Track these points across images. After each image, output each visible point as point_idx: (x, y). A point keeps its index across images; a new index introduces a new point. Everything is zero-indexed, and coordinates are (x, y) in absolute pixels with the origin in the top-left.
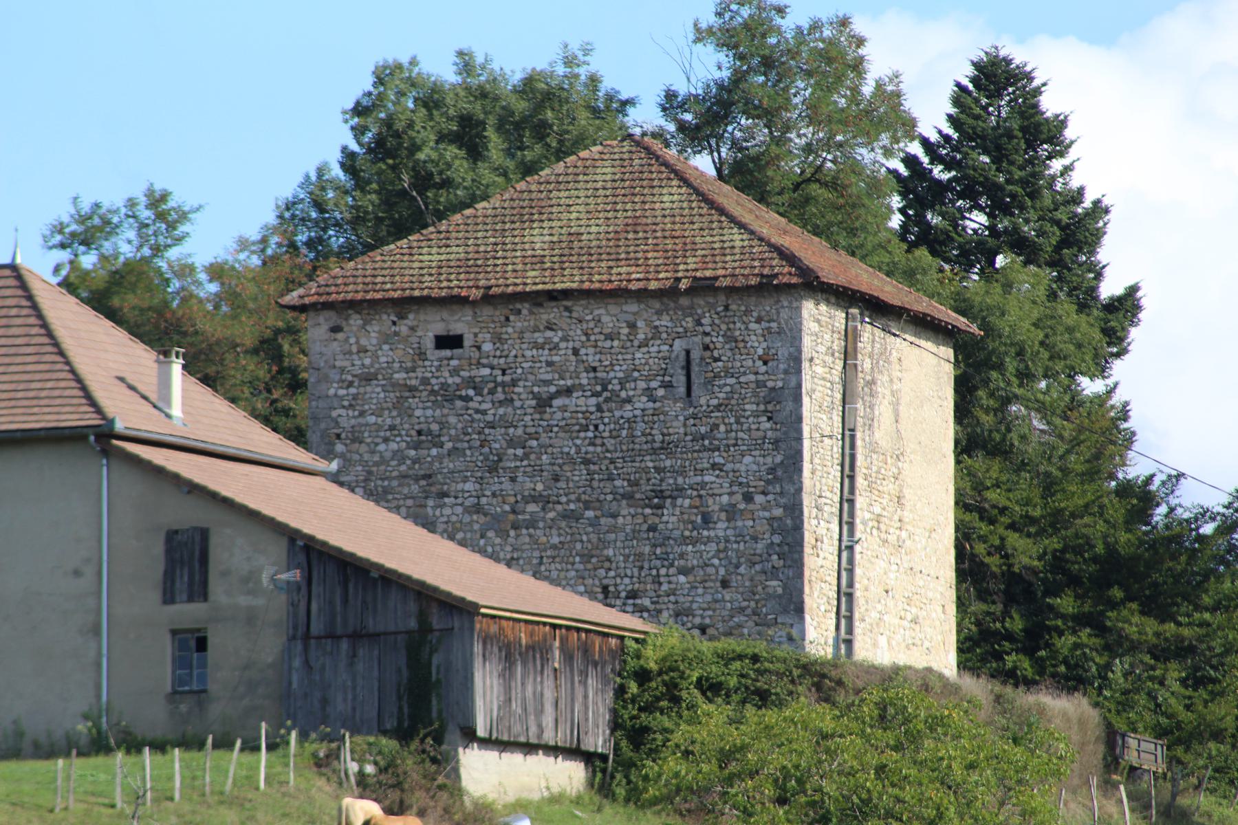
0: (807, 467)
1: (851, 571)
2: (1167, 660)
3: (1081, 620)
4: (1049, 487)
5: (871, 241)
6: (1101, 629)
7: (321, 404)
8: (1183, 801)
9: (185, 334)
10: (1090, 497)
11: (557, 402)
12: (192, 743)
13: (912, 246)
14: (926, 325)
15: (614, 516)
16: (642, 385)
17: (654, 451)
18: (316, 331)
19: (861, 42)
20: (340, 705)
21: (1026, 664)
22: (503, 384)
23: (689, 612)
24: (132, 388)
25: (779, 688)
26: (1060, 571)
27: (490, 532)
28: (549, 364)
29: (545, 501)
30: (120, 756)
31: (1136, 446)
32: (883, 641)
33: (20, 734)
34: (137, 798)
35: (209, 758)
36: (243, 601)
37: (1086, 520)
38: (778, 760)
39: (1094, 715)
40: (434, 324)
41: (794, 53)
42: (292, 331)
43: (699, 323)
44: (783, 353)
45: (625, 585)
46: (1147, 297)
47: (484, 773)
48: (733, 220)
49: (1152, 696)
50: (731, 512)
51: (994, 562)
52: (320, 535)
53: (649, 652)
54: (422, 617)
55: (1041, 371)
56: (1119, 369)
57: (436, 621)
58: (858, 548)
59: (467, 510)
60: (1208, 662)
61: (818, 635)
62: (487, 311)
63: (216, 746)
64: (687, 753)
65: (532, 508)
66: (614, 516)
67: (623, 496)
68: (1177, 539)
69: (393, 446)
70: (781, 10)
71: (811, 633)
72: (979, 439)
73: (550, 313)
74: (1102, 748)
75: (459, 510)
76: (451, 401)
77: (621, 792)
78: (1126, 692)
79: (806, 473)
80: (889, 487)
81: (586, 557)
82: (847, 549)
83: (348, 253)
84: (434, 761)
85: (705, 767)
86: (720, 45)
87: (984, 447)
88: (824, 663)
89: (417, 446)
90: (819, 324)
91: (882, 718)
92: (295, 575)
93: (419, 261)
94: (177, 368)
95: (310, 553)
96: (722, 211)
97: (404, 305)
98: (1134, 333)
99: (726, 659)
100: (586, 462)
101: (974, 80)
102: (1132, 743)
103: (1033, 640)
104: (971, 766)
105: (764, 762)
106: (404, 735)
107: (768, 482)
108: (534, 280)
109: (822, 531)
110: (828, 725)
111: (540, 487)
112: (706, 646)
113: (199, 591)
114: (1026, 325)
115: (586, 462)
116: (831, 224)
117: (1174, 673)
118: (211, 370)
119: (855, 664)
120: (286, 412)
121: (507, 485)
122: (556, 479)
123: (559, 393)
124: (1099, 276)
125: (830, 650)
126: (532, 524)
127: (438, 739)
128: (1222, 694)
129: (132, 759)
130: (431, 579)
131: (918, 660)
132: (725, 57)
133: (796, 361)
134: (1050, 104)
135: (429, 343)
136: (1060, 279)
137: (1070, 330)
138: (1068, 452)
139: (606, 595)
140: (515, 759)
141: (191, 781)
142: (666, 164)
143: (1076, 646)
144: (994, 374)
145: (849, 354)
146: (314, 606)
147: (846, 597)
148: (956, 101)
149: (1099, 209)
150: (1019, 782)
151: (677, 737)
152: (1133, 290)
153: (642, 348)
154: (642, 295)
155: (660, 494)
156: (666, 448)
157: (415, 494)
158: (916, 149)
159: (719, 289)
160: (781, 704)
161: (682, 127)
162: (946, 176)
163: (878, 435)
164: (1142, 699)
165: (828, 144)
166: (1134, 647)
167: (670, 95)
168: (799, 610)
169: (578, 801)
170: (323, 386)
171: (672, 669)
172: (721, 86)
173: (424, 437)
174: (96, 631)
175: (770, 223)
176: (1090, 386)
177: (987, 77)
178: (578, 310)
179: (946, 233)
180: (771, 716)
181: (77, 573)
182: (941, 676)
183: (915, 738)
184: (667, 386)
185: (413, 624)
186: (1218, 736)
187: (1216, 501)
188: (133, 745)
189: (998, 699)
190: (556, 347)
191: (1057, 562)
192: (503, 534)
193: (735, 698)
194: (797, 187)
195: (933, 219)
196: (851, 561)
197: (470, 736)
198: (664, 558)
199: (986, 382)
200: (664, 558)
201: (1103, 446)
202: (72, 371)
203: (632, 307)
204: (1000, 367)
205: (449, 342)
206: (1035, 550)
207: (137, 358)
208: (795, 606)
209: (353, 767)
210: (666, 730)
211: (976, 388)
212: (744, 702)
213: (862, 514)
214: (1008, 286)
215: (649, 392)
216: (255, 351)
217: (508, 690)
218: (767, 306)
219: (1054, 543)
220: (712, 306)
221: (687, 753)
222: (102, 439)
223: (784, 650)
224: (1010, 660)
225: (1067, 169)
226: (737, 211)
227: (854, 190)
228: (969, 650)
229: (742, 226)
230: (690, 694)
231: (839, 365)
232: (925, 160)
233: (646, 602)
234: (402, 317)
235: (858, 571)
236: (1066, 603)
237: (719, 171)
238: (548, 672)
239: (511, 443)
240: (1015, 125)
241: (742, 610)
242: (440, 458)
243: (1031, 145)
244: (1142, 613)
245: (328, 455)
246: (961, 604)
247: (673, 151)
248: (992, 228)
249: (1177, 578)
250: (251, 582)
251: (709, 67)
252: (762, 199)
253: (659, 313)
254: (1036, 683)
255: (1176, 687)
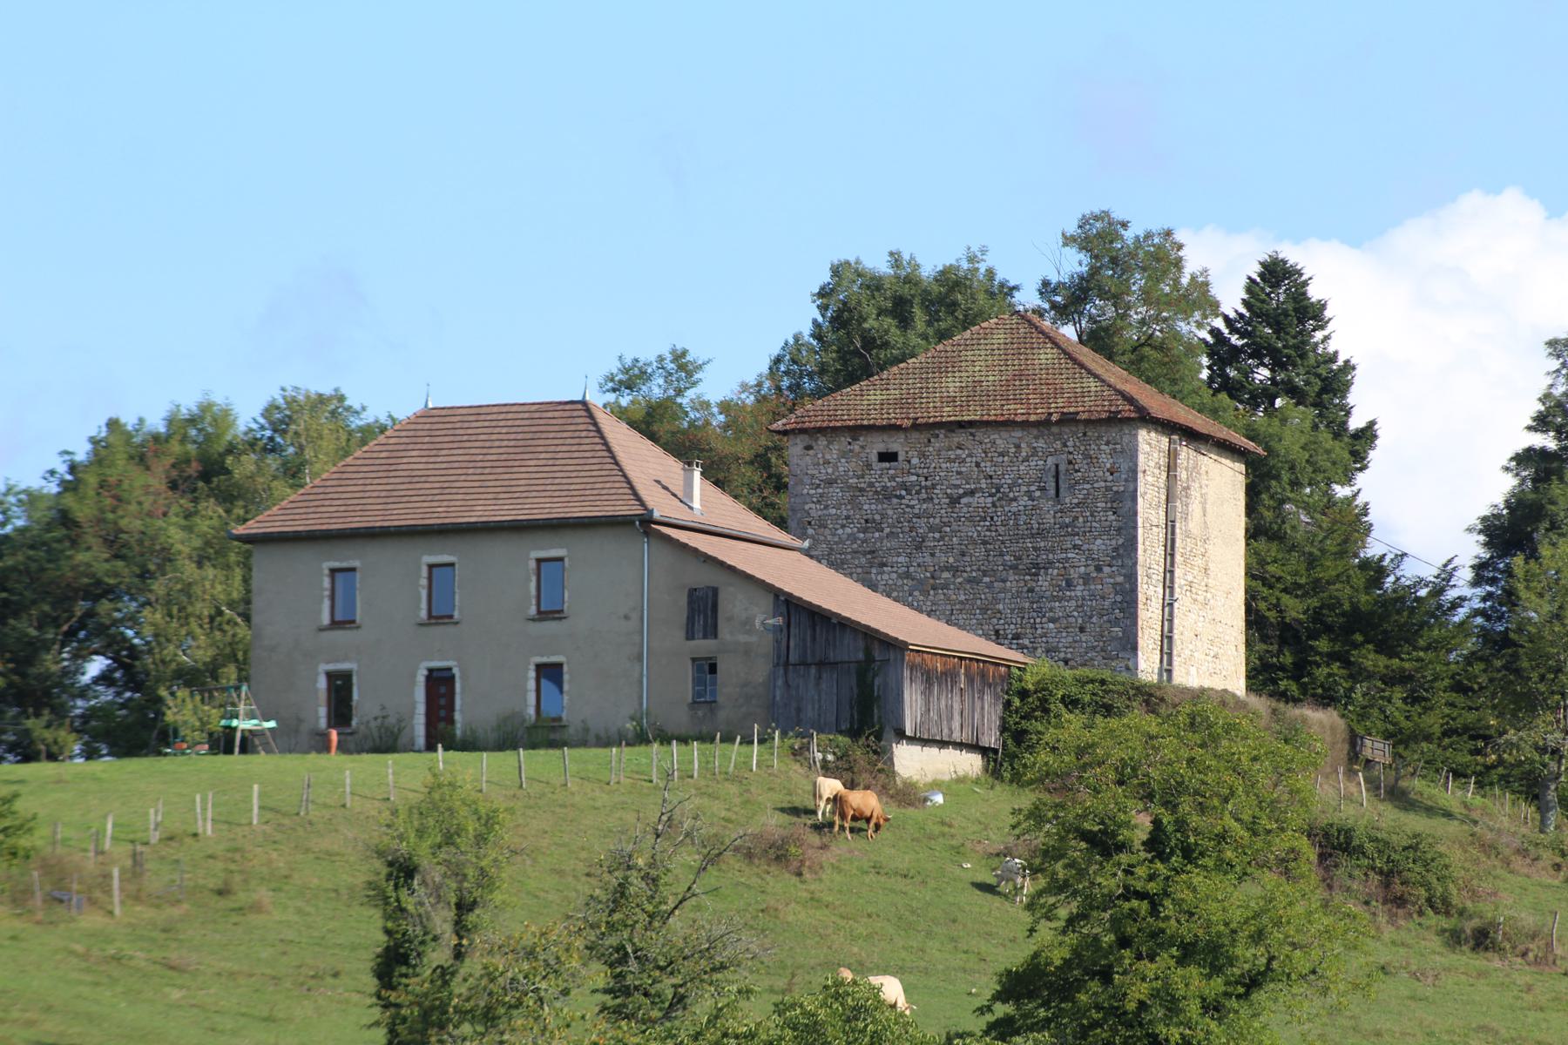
0: (1140, 547)
1: (1171, 621)
2: (1393, 685)
3: (1332, 657)
4: (1312, 562)
5: (1187, 388)
6: (1347, 663)
7: (798, 500)
8: (1403, 784)
9: (702, 450)
10: (1340, 569)
11: (964, 500)
12: (706, 738)
13: (1217, 391)
14: (1227, 448)
15: (1004, 581)
16: (1024, 488)
17: (1033, 536)
18: (794, 448)
19: (1180, 247)
20: (810, 713)
21: (1294, 687)
22: (926, 487)
23: (1056, 650)
24: (665, 488)
25: (1119, 703)
26: (1319, 622)
27: (917, 591)
28: (959, 473)
29: (955, 570)
30: (656, 746)
31: (1373, 534)
32: (1193, 670)
33: (586, 730)
34: (669, 776)
35: (718, 748)
36: (742, 638)
37: (1338, 586)
38: (1118, 753)
39: (1341, 724)
40: (878, 444)
41: (1132, 255)
42: (777, 449)
43: (1065, 445)
44: (1124, 467)
45: (1011, 630)
46: (1381, 429)
47: (910, 761)
48: (1089, 372)
49: (1382, 711)
50: (1086, 579)
51: (1272, 615)
52: (796, 594)
53: (1028, 677)
54: (868, 652)
55: (1306, 481)
56: (1361, 479)
57: (877, 655)
58: (1176, 605)
59: (900, 576)
60: (1421, 687)
61: (1147, 665)
62: (915, 435)
63: (722, 741)
64: (1054, 749)
65: (946, 575)
66: (1004, 581)
67: (1011, 567)
68: (1402, 599)
69: (848, 531)
70: (1124, 225)
71: (1142, 665)
72: (1262, 529)
73: (960, 437)
74: (1346, 747)
75: (894, 576)
76: (889, 498)
77: (1007, 775)
78: (1364, 708)
79: (1140, 552)
80: (1199, 561)
81: (984, 610)
82: (1169, 605)
83: (818, 394)
84: (875, 752)
85: (1067, 758)
86: (1081, 249)
87: (1266, 534)
88: (1152, 686)
89: (865, 531)
90: (1150, 447)
91: (1192, 724)
92: (779, 621)
93: (868, 400)
94: (697, 474)
95: (789, 605)
96: (1082, 366)
97: (856, 431)
98: (1372, 454)
99: (1082, 682)
100: (985, 543)
101: (1261, 275)
102: (1368, 743)
103: (1299, 671)
104: (1255, 759)
105: (1108, 755)
106: (854, 734)
107: (1113, 558)
108: (948, 414)
109: (1151, 592)
110: (1154, 730)
111: (951, 560)
112: (1068, 673)
113: (712, 631)
114: (1296, 448)
115: (985, 543)
116: (1159, 376)
117: (1398, 694)
118: (721, 476)
119: (1176, 688)
120: (772, 505)
121: (928, 559)
122: (963, 554)
123: (965, 494)
124: (1348, 413)
125: (1156, 677)
126: (945, 586)
127: (879, 737)
128: (1431, 709)
129: (665, 748)
130: (873, 625)
131: (1218, 684)
132: (1084, 258)
133: (1133, 473)
134: (1314, 293)
135: (874, 458)
136: (1320, 415)
137: (1328, 452)
138: (1326, 538)
139: (997, 637)
140: (935, 750)
141: (706, 764)
142: (1042, 332)
143: (1330, 675)
144: (1274, 483)
145: (1171, 467)
146: (792, 644)
147: (1167, 639)
148: (1249, 290)
149: (1348, 367)
150: (1288, 770)
151: (1047, 738)
152: (1372, 424)
153: (1026, 462)
154: (1025, 425)
155: (1036, 566)
156: (1041, 533)
157: (864, 565)
158: (1219, 323)
159: (1080, 421)
160: (1121, 715)
161: (1054, 306)
162: (1240, 343)
163: (1191, 525)
164: (1375, 712)
165: (1157, 319)
166: (1370, 676)
167: (1046, 283)
168: (1135, 648)
169: (977, 781)
170: (799, 488)
171: (1044, 689)
172: (1082, 278)
173: (870, 524)
174: (640, 658)
175: (1115, 374)
176: (1341, 491)
177: (1270, 272)
178: (979, 435)
179: (1240, 382)
180: (1114, 723)
181: (627, 617)
182: (1234, 695)
183: (1215, 739)
184: (1042, 489)
185: (861, 656)
186: (1428, 738)
187: (1429, 573)
188: (665, 739)
189: (1274, 711)
190: (964, 461)
191: (1317, 615)
192: (926, 593)
193: (1088, 710)
194: (1134, 349)
195: (1232, 373)
196: (1171, 614)
197: (901, 735)
198: (1039, 611)
199: (1268, 488)
200: (1039, 611)
201: (1350, 534)
202: (625, 476)
203: (1018, 434)
204: (1277, 477)
205: (888, 457)
206: (1301, 607)
207: (671, 468)
208: (1130, 645)
209: (819, 756)
210: (1039, 733)
211: (1260, 493)
212: (1094, 713)
213: (1178, 581)
214: (1284, 421)
215: (1029, 494)
216: (752, 463)
217: (927, 703)
218: (1113, 433)
219: (1314, 602)
220: (1075, 433)
221: (1054, 749)
222: (645, 524)
223: (1123, 677)
224: (1283, 684)
225: (1327, 338)
226: (1092, 366)
227: (1175, 352)
228: (1254, 677)
229: (1096, 376)
230: (1056, 707)
231: (1164, 475)
232: (1226, 331)
233: (1026, 642)
234: (855, 439)
235: (1176, 621)
236: (1323, 645)
237: (1080, 337)
238: (956, 690)
239: (931, 529)
240: (1290, 306)
241: (1094, 648)
242: (881, 539)
243: (1301, 321)
244: (1376, 652)
245: (803, 537)
246: (1248, 644)
247: (1047, 323)
248: (1273, 379)
249: (1401, 627)
250: (748, 628)
251: (1074, 263)
252: (1110, 358)
253: (1036, 438)
254: (1300, 700)
255: (1399, 704)
